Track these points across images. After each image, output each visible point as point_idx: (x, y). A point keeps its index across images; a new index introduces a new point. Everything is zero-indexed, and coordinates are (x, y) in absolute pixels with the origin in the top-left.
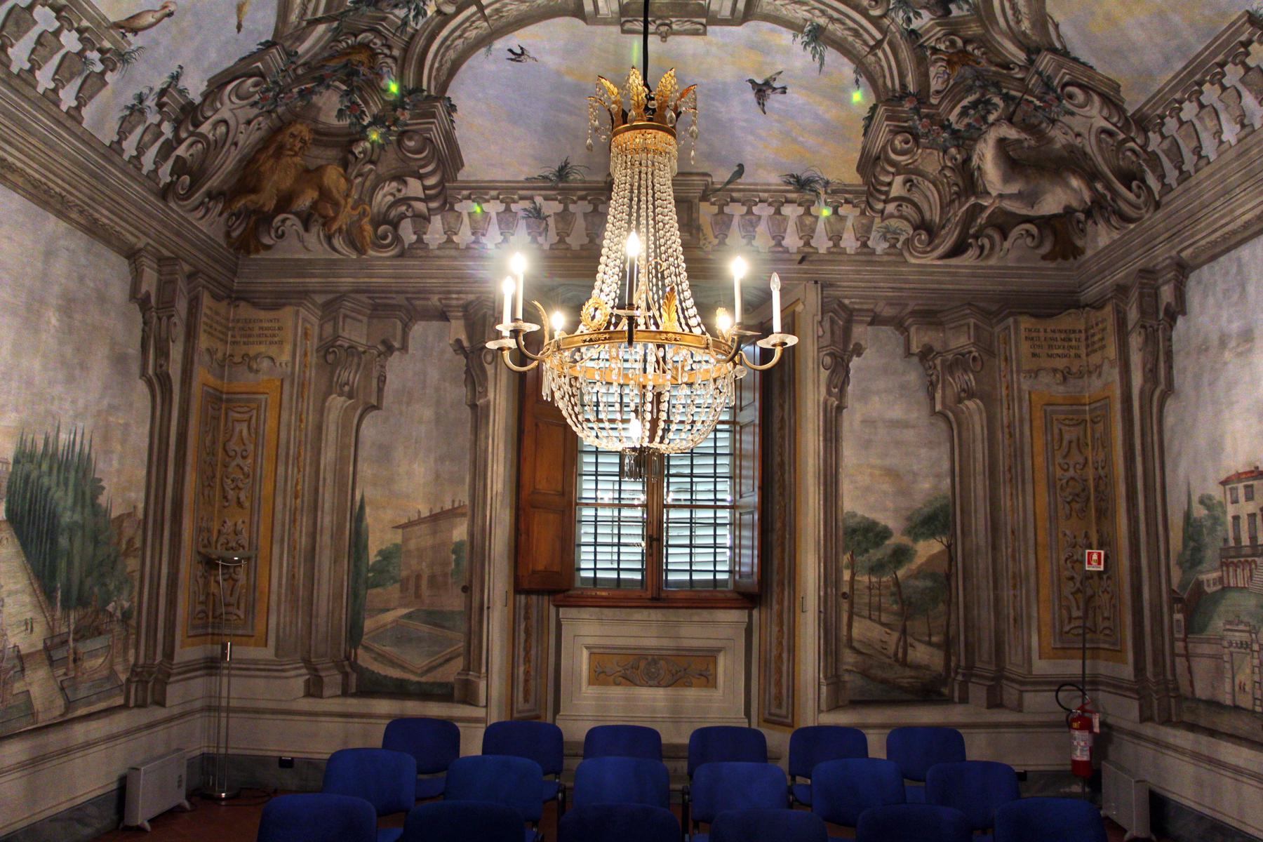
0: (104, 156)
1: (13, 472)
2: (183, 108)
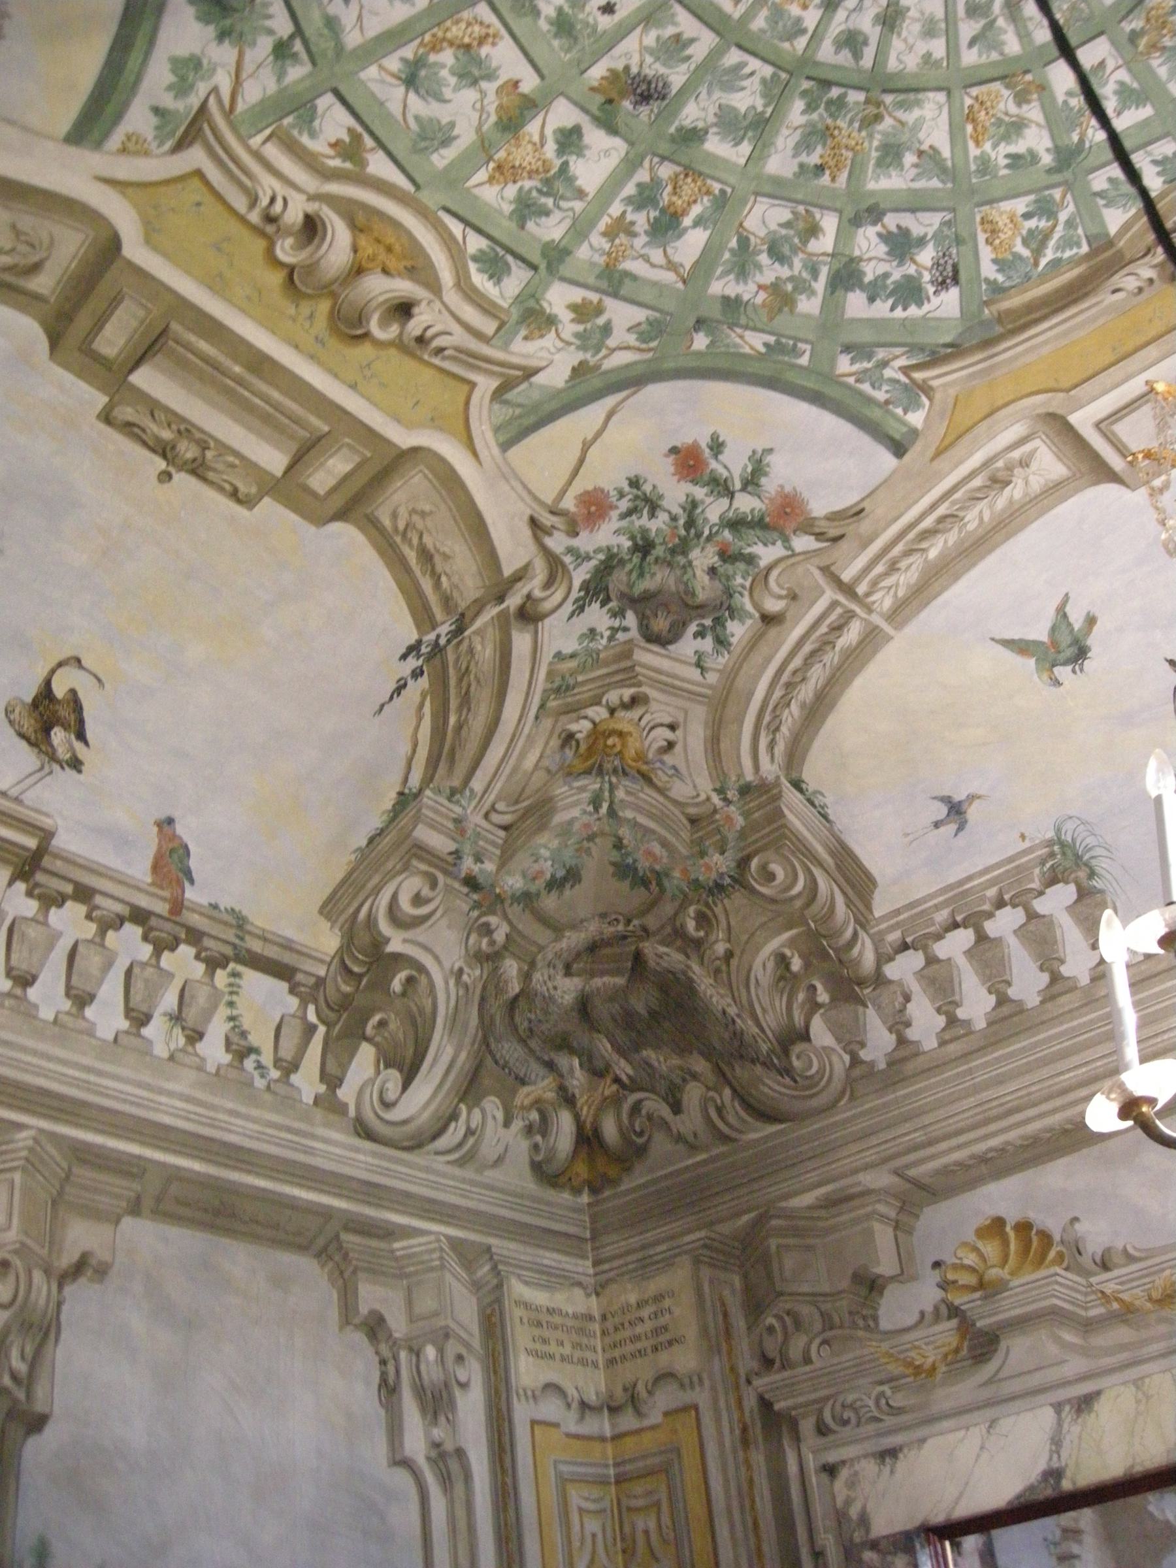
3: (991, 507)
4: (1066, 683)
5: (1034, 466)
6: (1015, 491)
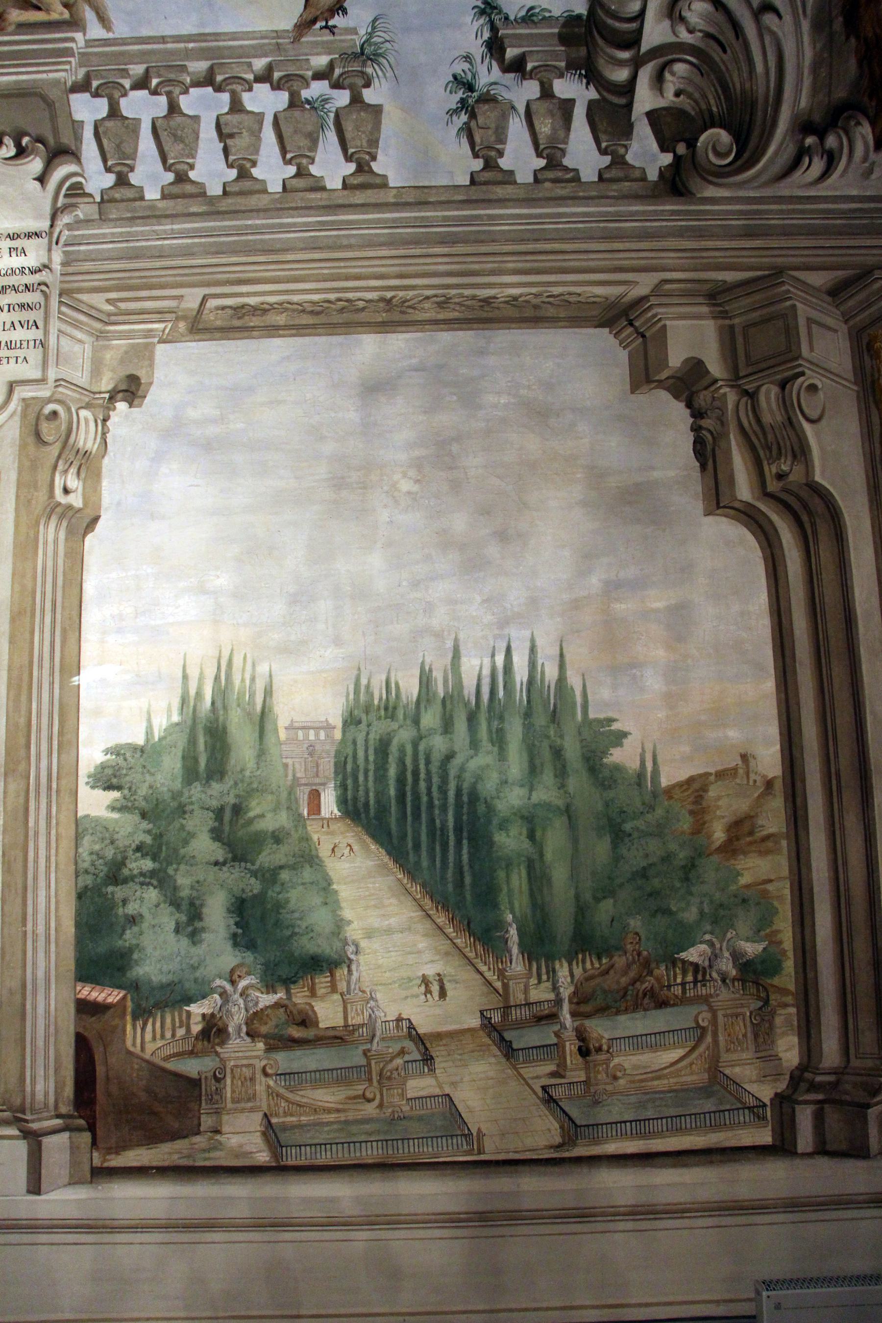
0: (468, 203)
1: (343, 741)
2: (564, 39)
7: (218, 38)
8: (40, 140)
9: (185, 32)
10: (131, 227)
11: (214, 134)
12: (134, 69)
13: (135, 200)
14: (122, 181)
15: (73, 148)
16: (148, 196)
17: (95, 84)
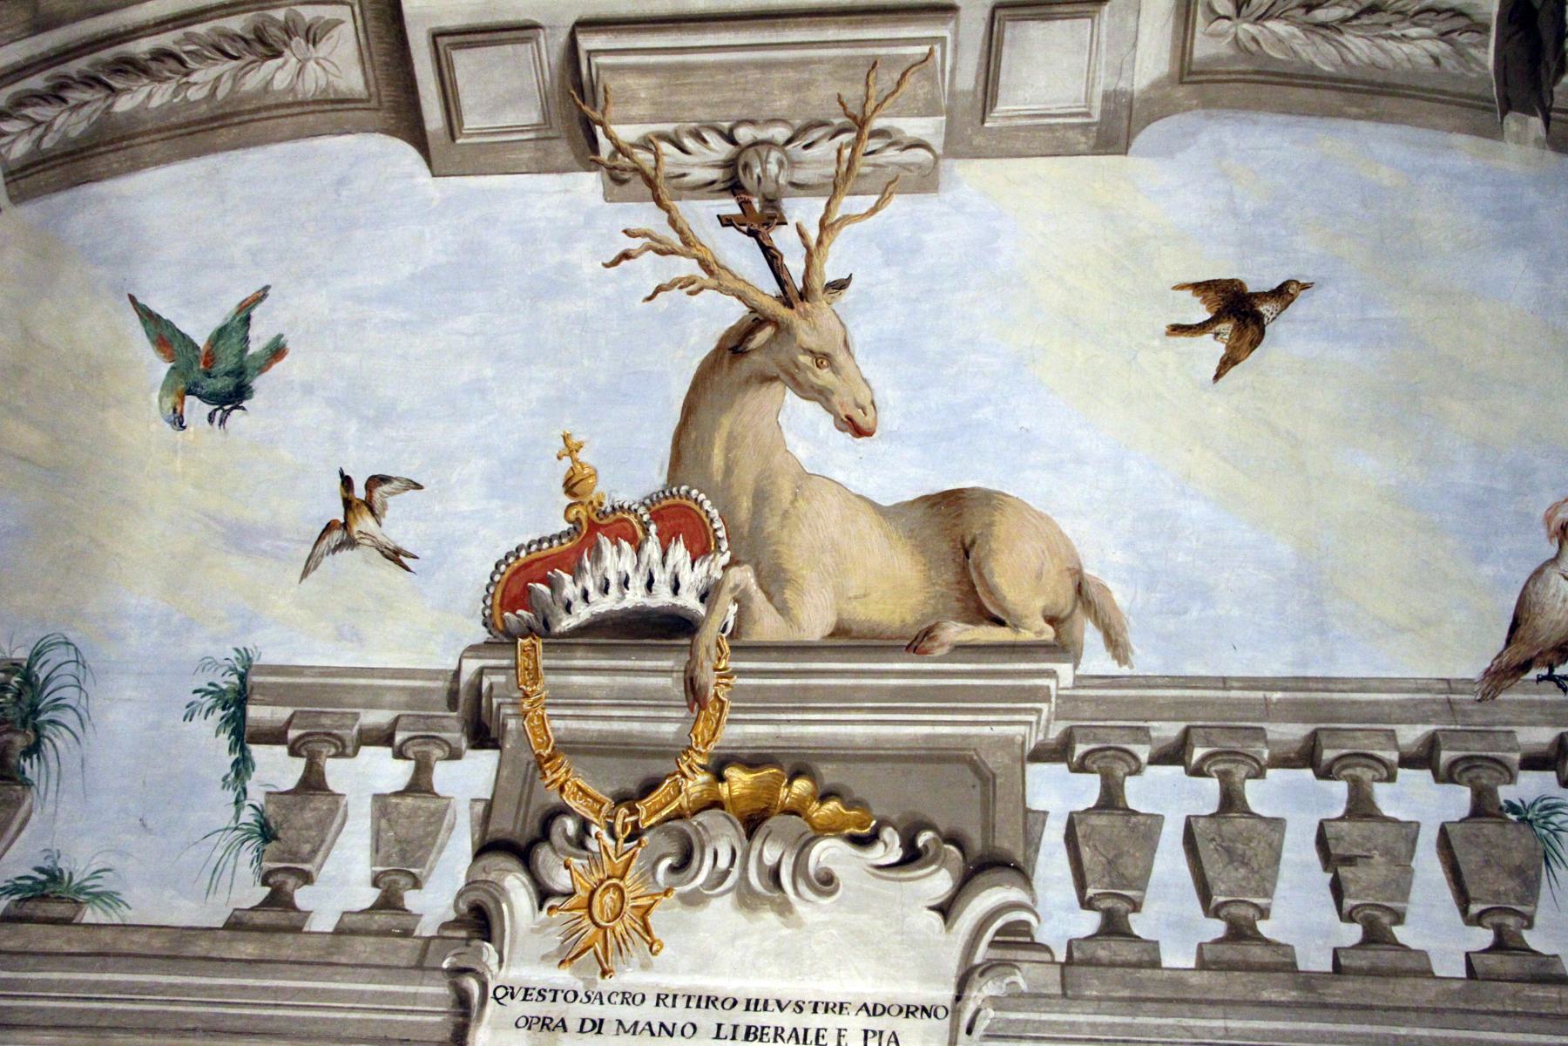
3: (236, 79)
4: (191, 429)
5: (323, 49)
6: (278, 75)
7: (1331, 686)
8: (955, 839)
9: (1267, 674)
10: (1134, 1015)
11: (1313, 856)
12: (1159, 729)
13: (1139, 965)
14: (1114, 927)
15: (1020, 859)
16: (1168, 960)
17: (1080, 749)
